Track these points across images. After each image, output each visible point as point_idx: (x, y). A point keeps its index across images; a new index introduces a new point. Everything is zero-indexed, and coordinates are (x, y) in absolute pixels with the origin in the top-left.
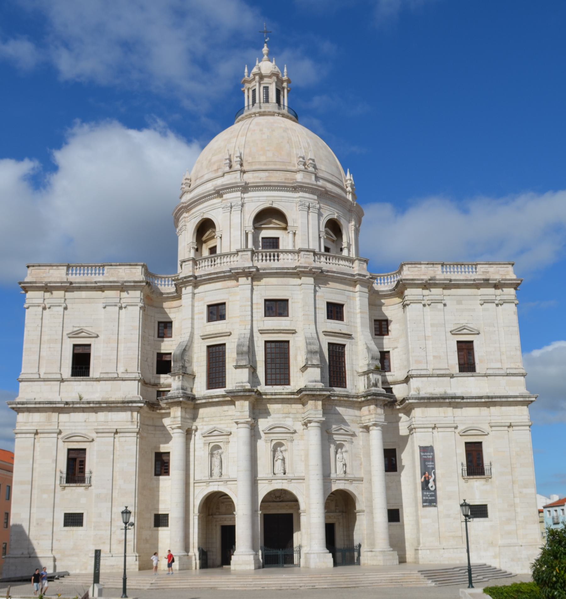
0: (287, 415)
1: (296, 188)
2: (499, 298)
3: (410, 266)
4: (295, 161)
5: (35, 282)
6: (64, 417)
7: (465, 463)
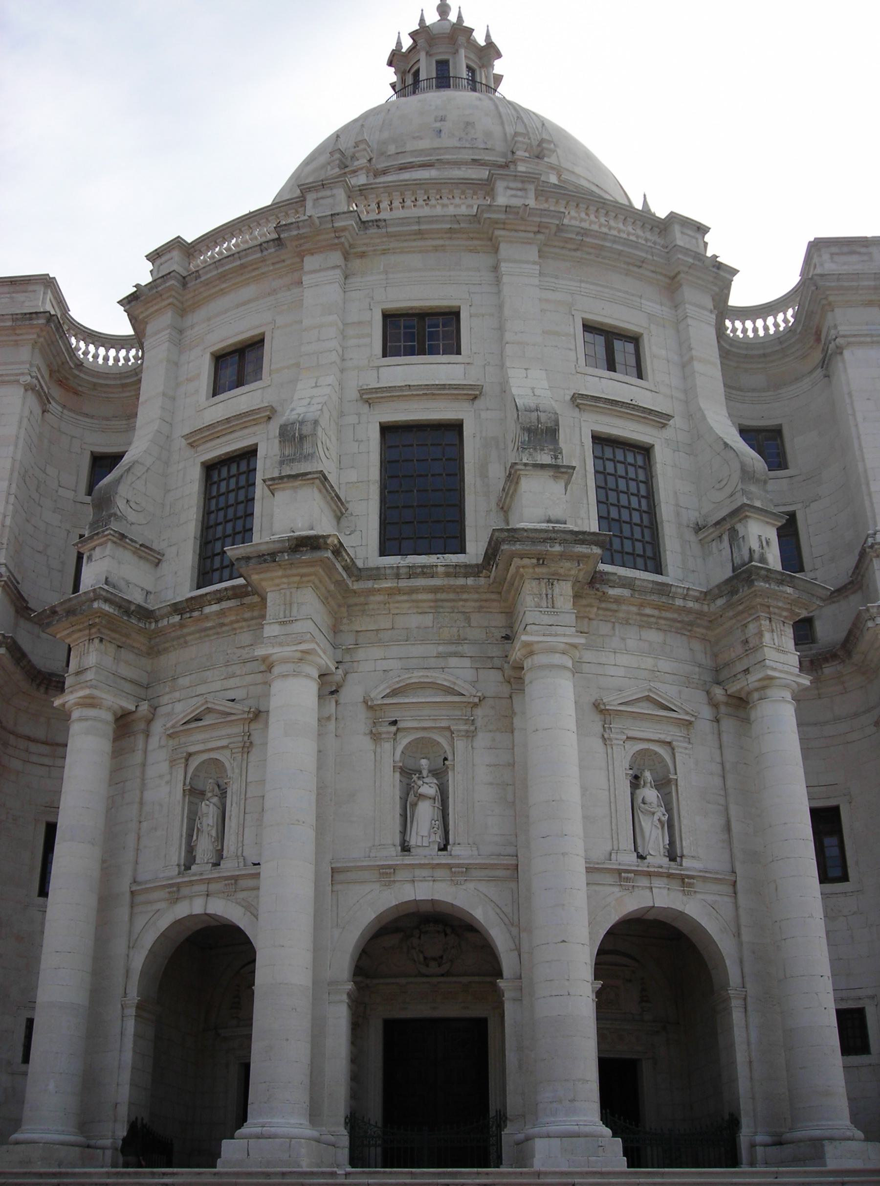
0: (452, 648)
3: (834, 250)
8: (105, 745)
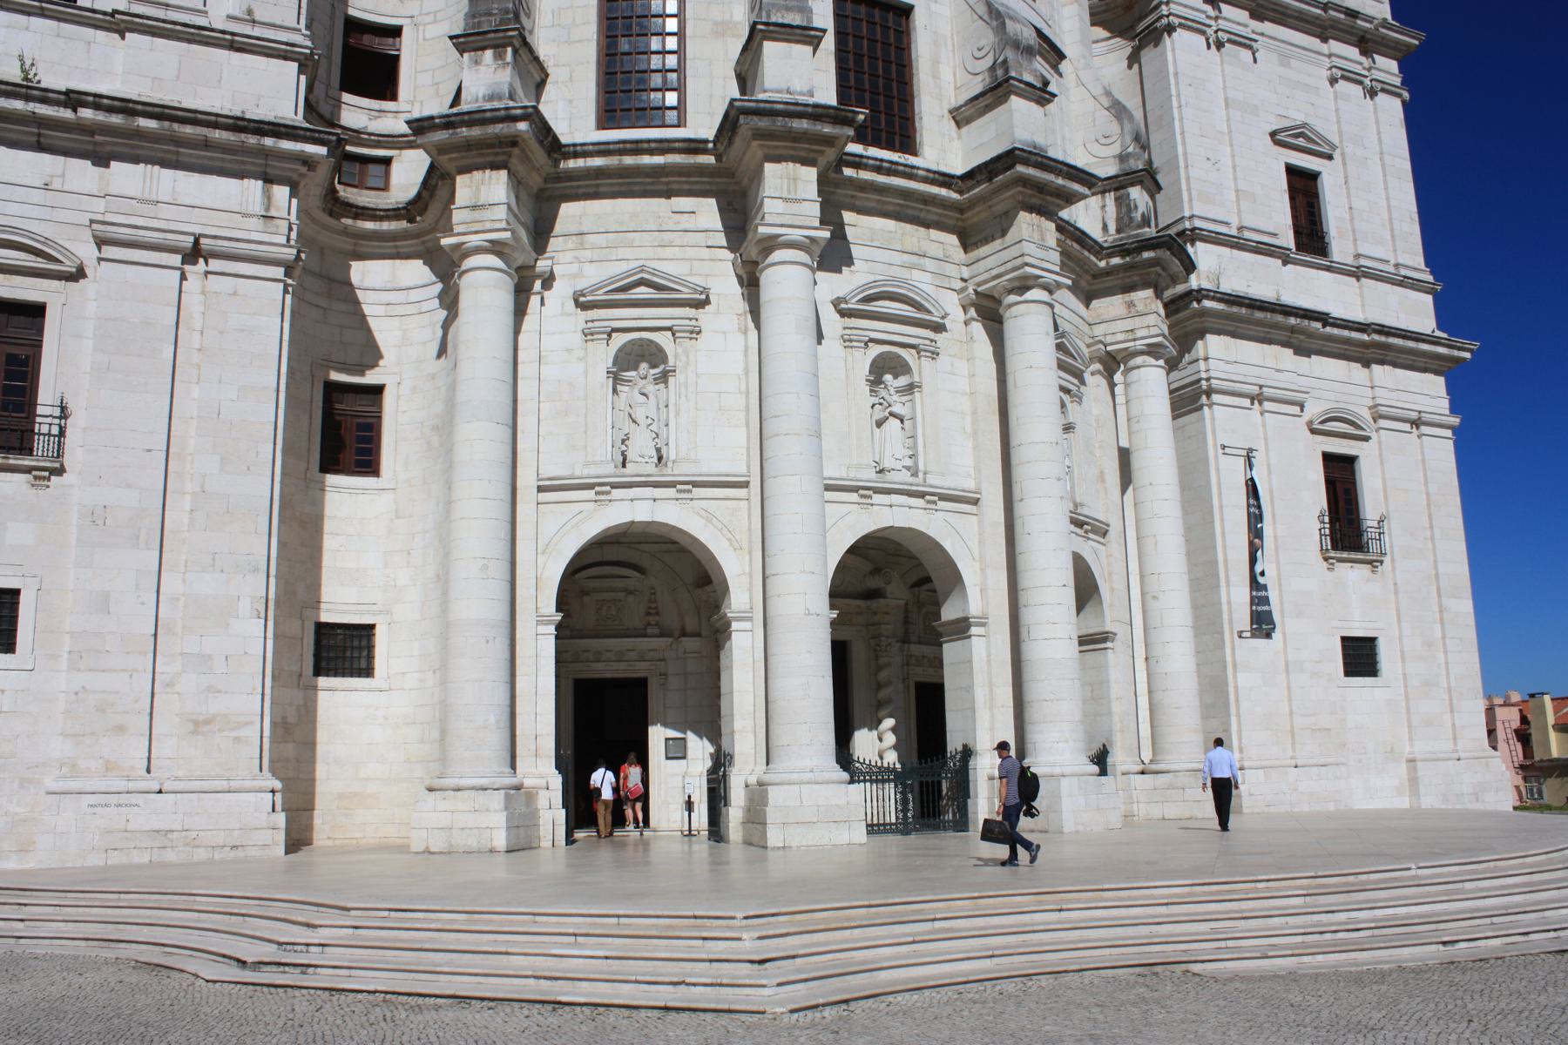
0: (915, 259)
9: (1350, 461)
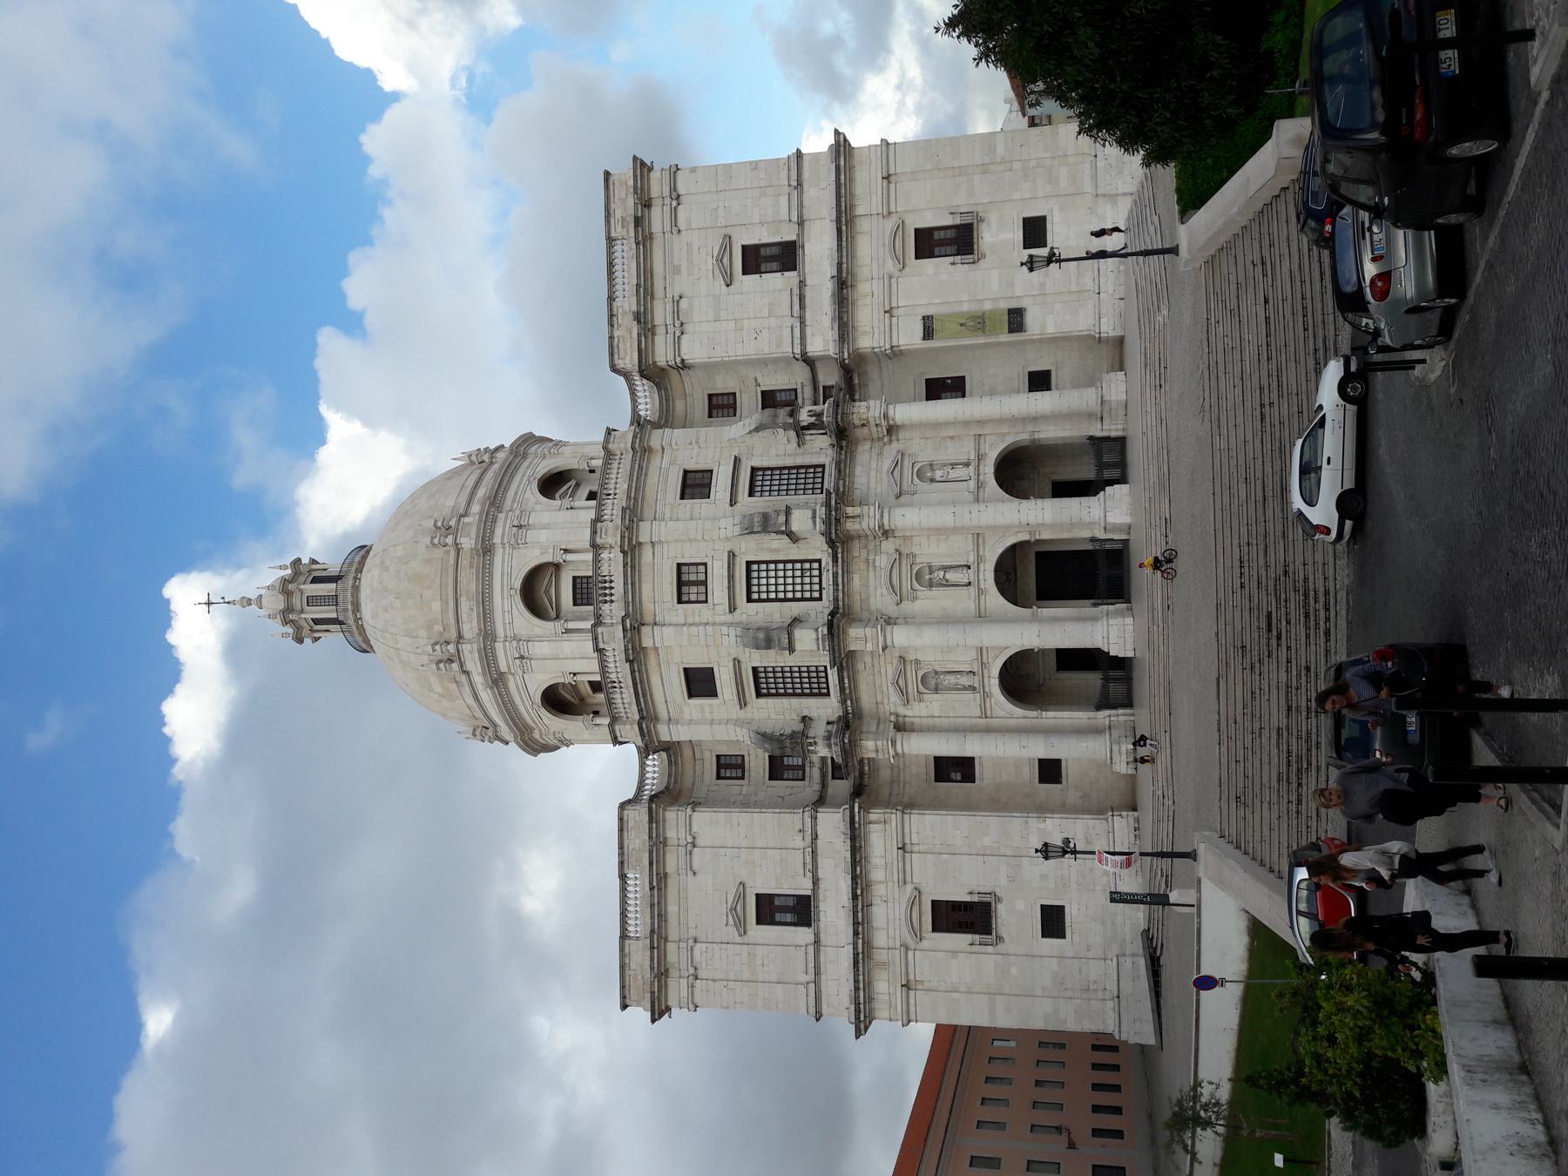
1: (486, 549)
2: (667, 201)
4: (439, 553)
5: (652, 993)
6: (880, 939)
7: (951, 259)
8: (914, 735)
9: (919, 233)
